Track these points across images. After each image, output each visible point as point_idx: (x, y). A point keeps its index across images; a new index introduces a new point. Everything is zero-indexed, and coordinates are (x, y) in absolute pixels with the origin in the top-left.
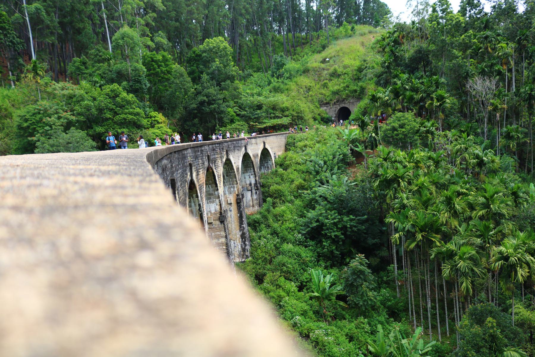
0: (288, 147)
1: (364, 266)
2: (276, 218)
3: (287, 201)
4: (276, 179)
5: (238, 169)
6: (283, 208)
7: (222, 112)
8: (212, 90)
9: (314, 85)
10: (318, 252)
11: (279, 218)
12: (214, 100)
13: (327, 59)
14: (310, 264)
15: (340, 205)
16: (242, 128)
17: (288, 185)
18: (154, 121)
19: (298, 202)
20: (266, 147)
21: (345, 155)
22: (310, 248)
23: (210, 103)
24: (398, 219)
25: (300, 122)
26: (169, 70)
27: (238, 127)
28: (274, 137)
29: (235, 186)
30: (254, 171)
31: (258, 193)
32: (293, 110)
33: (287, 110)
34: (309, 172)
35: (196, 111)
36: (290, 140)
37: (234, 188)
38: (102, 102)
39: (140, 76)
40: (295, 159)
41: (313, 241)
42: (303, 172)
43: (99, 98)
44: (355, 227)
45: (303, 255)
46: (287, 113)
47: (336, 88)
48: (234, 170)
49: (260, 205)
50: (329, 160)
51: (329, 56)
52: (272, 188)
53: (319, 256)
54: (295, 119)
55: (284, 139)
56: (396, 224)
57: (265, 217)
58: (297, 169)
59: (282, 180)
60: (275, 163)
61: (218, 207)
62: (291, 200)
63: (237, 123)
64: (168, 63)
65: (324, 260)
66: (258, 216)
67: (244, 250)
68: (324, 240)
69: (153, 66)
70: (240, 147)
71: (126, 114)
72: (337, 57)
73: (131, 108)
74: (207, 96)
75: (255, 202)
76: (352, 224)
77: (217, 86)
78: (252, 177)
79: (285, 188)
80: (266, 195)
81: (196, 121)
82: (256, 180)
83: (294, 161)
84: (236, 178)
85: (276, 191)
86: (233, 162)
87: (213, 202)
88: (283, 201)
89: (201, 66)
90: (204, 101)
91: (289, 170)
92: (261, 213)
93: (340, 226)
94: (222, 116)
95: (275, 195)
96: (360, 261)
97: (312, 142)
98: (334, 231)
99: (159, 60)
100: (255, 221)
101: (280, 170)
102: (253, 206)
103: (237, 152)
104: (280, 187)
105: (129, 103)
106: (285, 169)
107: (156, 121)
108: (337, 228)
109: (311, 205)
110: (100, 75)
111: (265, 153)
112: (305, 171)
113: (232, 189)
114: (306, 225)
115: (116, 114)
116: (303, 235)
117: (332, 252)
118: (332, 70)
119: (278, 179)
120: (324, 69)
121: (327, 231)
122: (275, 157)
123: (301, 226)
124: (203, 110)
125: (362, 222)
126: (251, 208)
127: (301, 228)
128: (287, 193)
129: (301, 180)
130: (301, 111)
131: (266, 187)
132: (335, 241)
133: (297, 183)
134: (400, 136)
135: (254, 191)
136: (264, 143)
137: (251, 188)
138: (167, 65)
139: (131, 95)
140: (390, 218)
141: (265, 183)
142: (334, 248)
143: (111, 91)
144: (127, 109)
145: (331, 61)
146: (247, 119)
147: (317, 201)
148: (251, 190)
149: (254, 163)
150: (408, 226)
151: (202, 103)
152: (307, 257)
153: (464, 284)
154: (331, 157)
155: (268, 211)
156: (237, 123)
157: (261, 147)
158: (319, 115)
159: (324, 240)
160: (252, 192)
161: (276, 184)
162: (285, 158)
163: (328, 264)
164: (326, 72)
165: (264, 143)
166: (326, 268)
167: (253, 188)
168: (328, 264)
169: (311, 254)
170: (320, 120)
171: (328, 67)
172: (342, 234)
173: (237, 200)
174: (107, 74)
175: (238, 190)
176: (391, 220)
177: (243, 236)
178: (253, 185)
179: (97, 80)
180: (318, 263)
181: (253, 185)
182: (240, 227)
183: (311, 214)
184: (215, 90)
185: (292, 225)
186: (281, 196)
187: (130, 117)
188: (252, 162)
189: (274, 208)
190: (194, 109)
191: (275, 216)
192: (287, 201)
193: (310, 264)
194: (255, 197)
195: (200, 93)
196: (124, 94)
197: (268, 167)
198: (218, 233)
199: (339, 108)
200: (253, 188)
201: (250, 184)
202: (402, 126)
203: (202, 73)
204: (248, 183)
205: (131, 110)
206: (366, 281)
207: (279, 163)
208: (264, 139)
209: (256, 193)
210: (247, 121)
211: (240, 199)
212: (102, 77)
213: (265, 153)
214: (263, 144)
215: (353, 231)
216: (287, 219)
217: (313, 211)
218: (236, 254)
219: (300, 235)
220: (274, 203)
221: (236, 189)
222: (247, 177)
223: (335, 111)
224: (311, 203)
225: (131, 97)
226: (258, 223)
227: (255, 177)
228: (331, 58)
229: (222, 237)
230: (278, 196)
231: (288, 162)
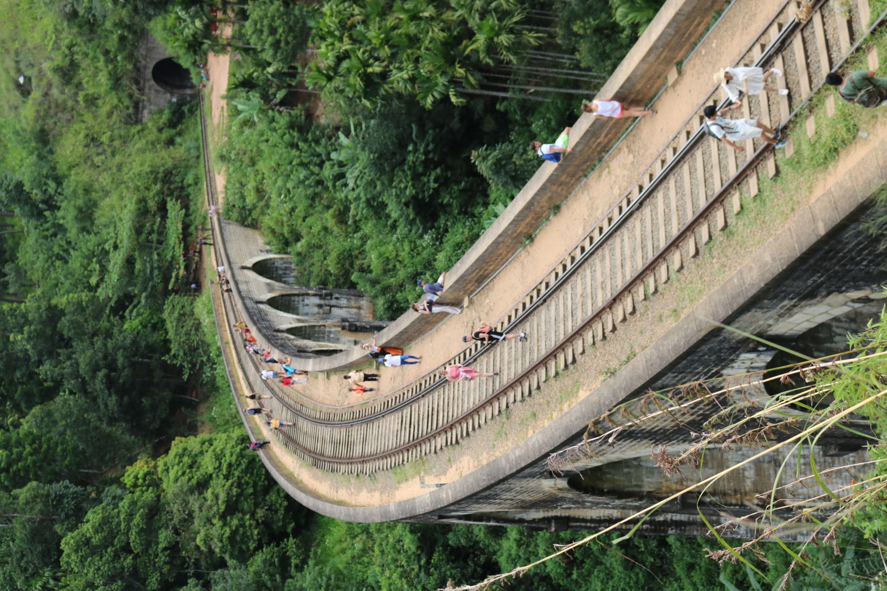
0: (247, 219)
1: (490, 154)
2: (389, 270)
3: (362, 245)
4: (316, 259)
5: (299, 321)
6: (373, 256)
7: (134, 342)
8: (84, 356)
9: (83, 126)
10: (459, 214)
11: (390, 266)
12: (105, 357)
13: (21, 80)
14: (475, 231)
15: (387, 161)
16: (179, 307)
17: (330, 239)
18: (144, 479)
19: (367, 228)
20: (250, 265)
21: (291, 126)
22: (449, 224)
23: (112, 366)
24: (429, 90)
25: (178, 179)
26: (29, 440)
27: (176, 314)
28: (228, 245)
29: (327, 329)
30: (298, 295)
31: (337, 295)
32: (147, 189)
33: (146, 202)
34: (314, 197)
35: (126, 399)
36: (235, 215)
37: (330, 332)
38: (99, 569)
39: (48, 495)
40: (281, 215)
41: (439, 217)
42: (311, 206)
43: (90, 575)
44: (427, 145)
45: (458, 238)
46: (152, 205)
47: (103, 78)
48: (301, 327)
49: (360, 295)
50: (300, 156)
51: (13, 73)
52: (332, 269)
53: (466, 213)
54: (169, 189)
56: (436, 94)
57: (385, 290)
58: (302, 214)
59: (320, 247)
60: (279, 253)
62: (361, 238)
63: (165, 315)
64: (14, 439)
65: (473, 206)
66: (381, 302)
68: (440, 201)
69: (19, 470)
70: (260, 311)
71: (129, 529)
72: (21, 57)
73: (118, 516)
74: (95, 369)
75: (353, 303)
76: (422, 150)
77: (72, 347)
78: (306, 301)
79: (336, 245)
80: (342, 280)
81: (146, 402)
82: (315, 295)
83: (285, 219)
84: (314, 326)
85: (338, 263)
86: (290, 326)
88: (360, 253)
89: (18, 374)
90: (107, 376)
91: (304, 231)
92: (376, 297)
93: (421, 170)
94: (143, 343)
95: (347, 265)
96: (480, 159)
97: (252, 176)
98: (428, 181)
99: (7, 456)
100: (389, 308)
101: (300, 246)
102: (359, 308)
104: (333, 255)
105: (105, 521)
106: (298, 238)
107: (145, 475)
108: (424, 174)
109: (377, 208)
110: (27, 578)
111: (261, 268)
112: (310, 202)
113: (332, 336)
114: (412, 223)
115: (127, 549)
116: (425, 231)
117: (462, 191)
118: (56, 79)
119: (317, 255)
120: (46, 95)
121: (426, 193)
122: (268, 251)
123: (410, 231)
124: (124, 383)
125: (422, 133)
126: (362, 312)
127: (413, 231)
128: (347, 244)
129: (328, 215)
130: (152, 172)
131: (326, 279)
132: (444, 183)
133: (331, 223)
134: (290, 39)
135: (333, 302)
136: (244, 268)
137: (326, 305)
138: (19, 443)
139: (90, 515)
140: (426, 101)
141: (318, 280)
142: (456, 188)
143: (76, 551)
144: (119, 524)
145: (28, 73)
146: (159, 296)
147: (374, 198)
148: (331, 306)
149: (284, 293)
150: (442, 80)
151: (110, 383)
152: (463, 232)
153: (532, 40)
154: (294, 152)
155: (374, 282)
156: (165, 315)
157: (252, 275)
158: (160, 130)
159: (440, 201)
160: (334, 306)
161: (325, 259)
162: (273, 232)
163: (480, 200)
164: (55, 92)
165: (244, 268)
166: (486, 205)
167: (327, 302)
168: (480, 200)
169: (460, 225)
170: (173, 132)
171: (45, 82)
172: (435, 168)
173: (350, 330)
174: (27, 562)
175: (335, 326)
176: (430, 100)
178: (322, 302)
179: (40, 583)
180: (475, 217)
181: (322, 302)
183: (394, 210)
184: (83, 351)
185: (407, 247)
186: (350, 256)
187: (137, 519)
188: (282, 296)
189: (371, 272)
190: (120, 404)
191: (386, 272)
192: (362, 245)
193: (475, 231)
194: (343, 302)
195: (84, 383)
196: (86, 528)
197: (286, 269)
199: (152, 82)
200: (327, 302)
202: (273, 31)
203: (32, 375)
204: (316, 310)
205: (122, 517)
206: (511, 156)
207: (280, 246)
209: (337, 298)
210: (166, 293)
211: (351, 325)
212: (33, 575)
213: (261, 268)
214: (246, 271)
215: (434, 150)
216: (394, 253)
217: (390, 207)
219: (426, 237)
220: (362, 270)
221: (333, 329)
222: (306, 309)
223: (157, 91)
224: (373, 207)
225: (93, 516)
226: (392, 303)
227: (308, 294)
228: (19, 71)
230: (348, 259)
231: (286, 230)
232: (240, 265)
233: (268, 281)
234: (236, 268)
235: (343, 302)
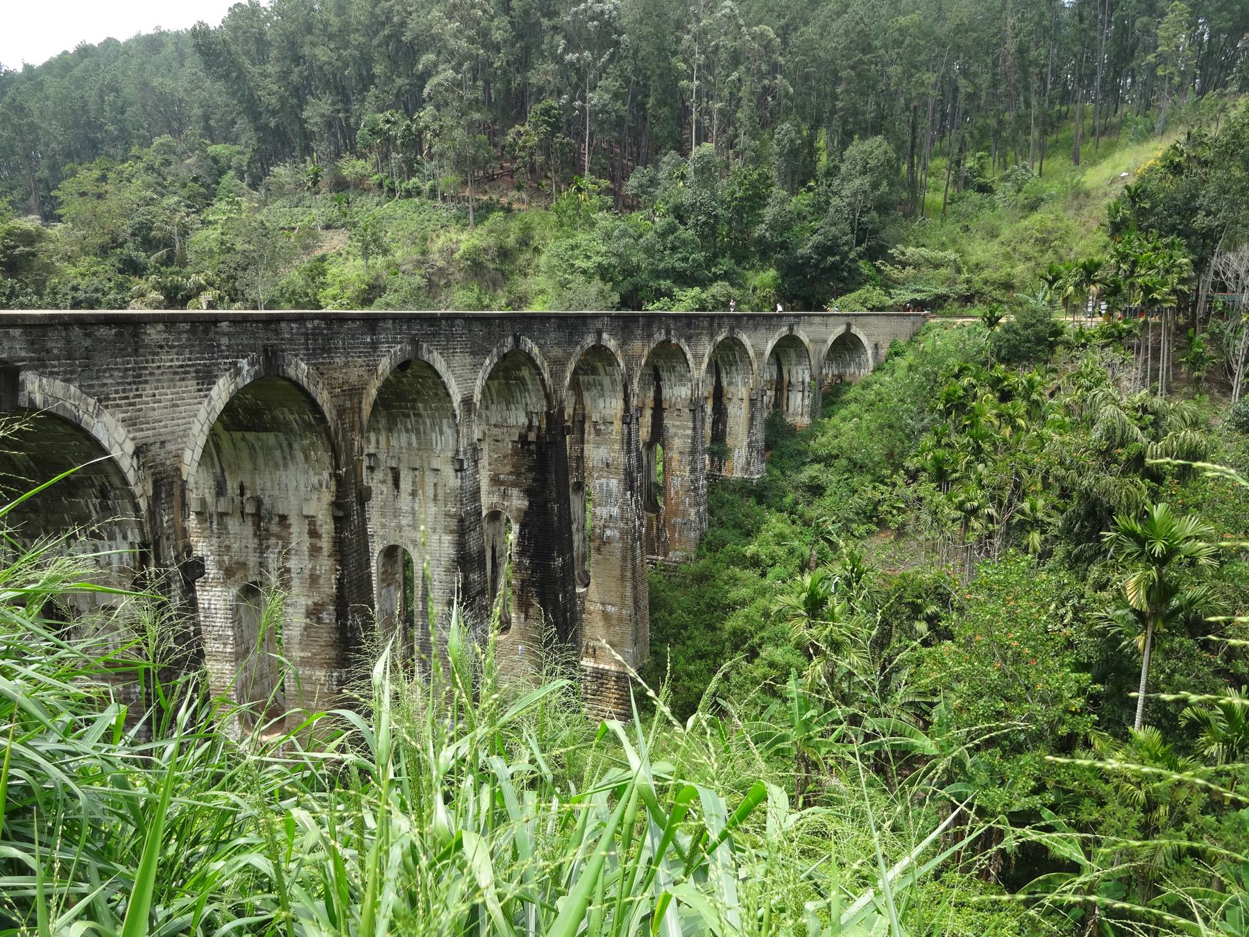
20: (853, 331)
28: (884, 319)
67: (748, 463)
70: (779, 326)
103: (762, 332)
135: (806, 394)
136: (849, 326)
148: (803, 391)
157: (841, 330)
165: (849, 326)
177: (750, 445)
200: (807, 389)
201: (803, 383)
218: (740, 466)
222: (800, 372)
233: (830, 342)
234: (850, 320)
235: (807, 402)
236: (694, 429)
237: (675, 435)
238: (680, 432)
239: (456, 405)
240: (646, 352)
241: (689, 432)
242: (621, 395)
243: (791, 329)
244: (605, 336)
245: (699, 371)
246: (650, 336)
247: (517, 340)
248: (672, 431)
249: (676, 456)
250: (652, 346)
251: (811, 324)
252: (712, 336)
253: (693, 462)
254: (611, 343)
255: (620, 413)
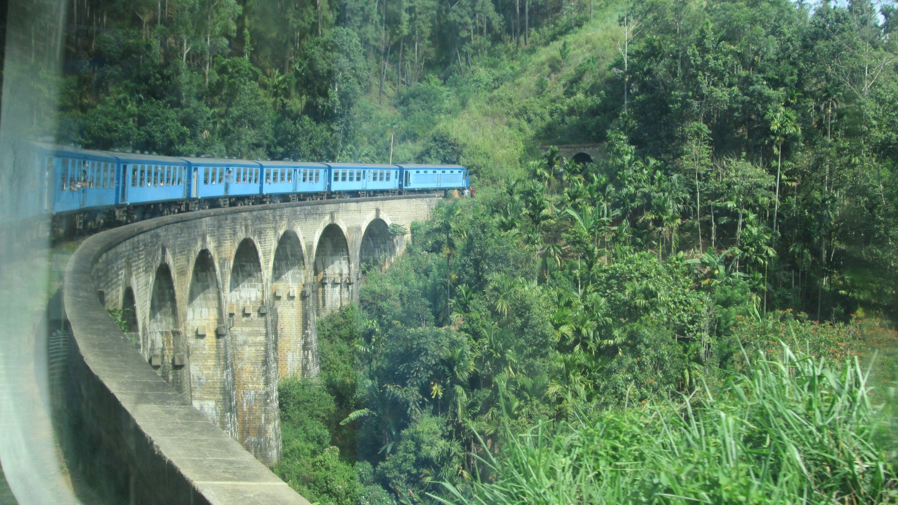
5: (310, 248)
20: (384, 216)
55: (426, 206)
61: (260, 294)
70: (322, 215)
87: (254, 286)
103: (310, 221)
136: (378, 211)
157: (370, 217)
165: (378, 211)
177: (305, 347)
182: (304, 333)
198: (257, 328)
204: (337, 271)
208: (379, 204)
229: (261, 334)
232: (381, 208)
233: (363, 230)
236: (267, 335)
237: (245, 343)
238: (251, 339)
239: (140, 333)
240: (234, 253)
241: (262, 339)
242: (215, 303)
243: (332, 217)
244: (208, 239)
245: (267, 270)
246: (235, 233)
247: (164, 252)
248: (240, 339)
249: (248, 367)
250: (237, 245)
251: (347, 211)
252: (275, 229)
253: (266, 372)
254: (211, 246)
255: (213, 326)
